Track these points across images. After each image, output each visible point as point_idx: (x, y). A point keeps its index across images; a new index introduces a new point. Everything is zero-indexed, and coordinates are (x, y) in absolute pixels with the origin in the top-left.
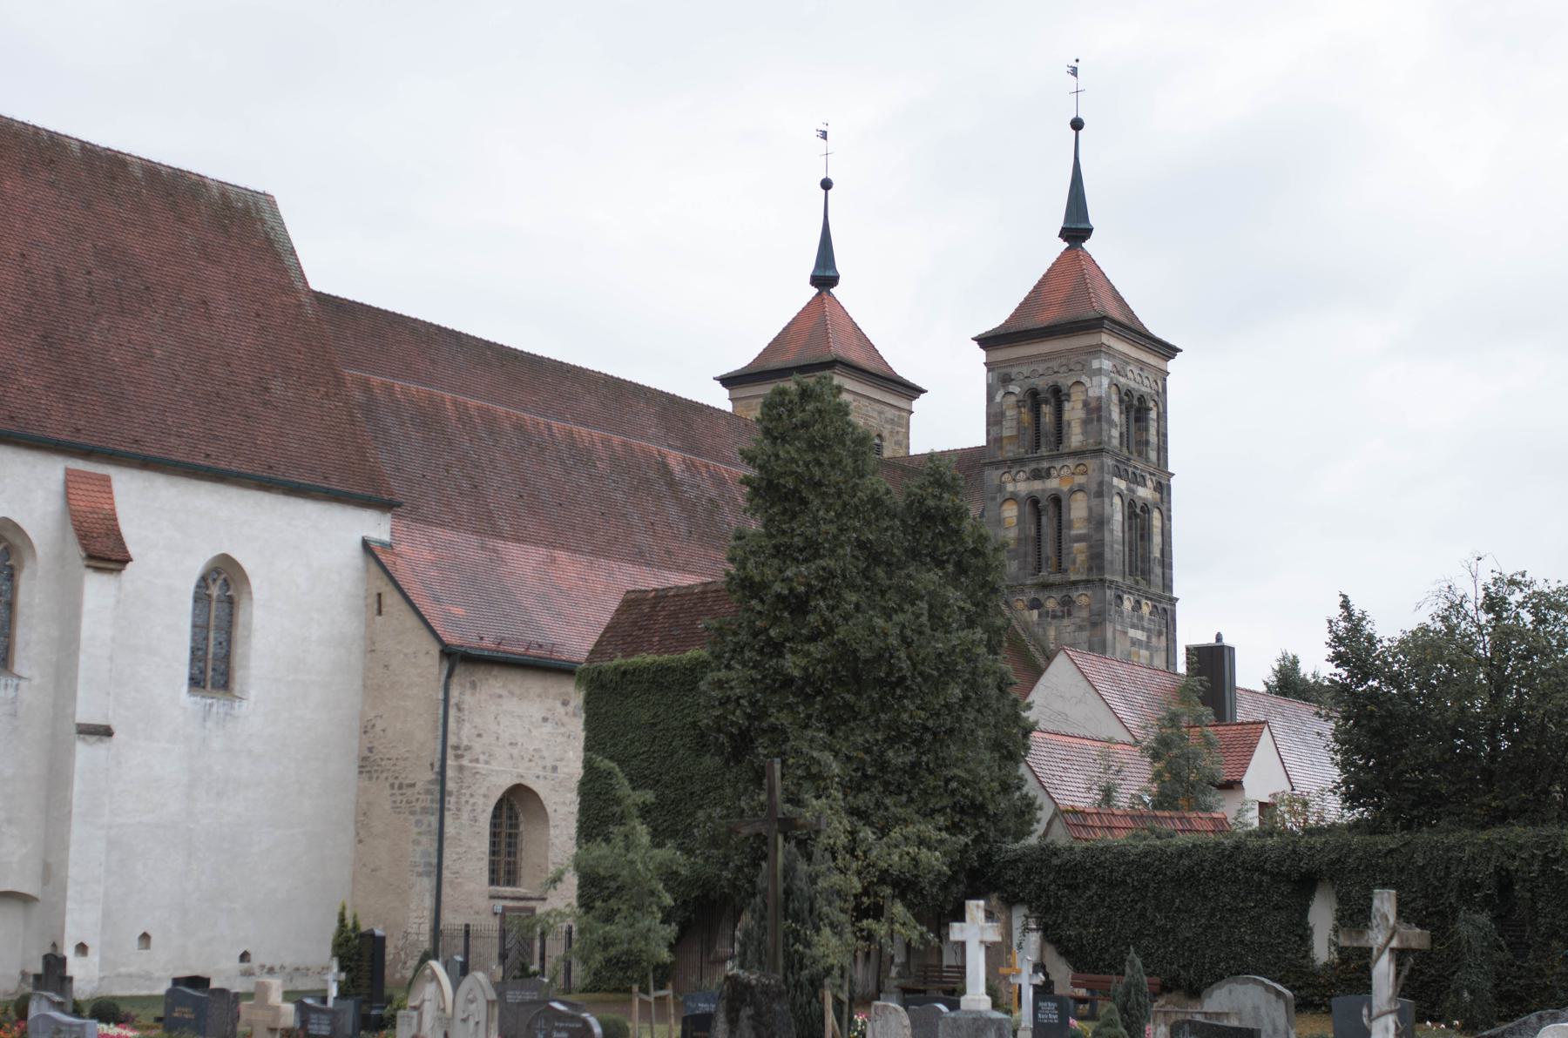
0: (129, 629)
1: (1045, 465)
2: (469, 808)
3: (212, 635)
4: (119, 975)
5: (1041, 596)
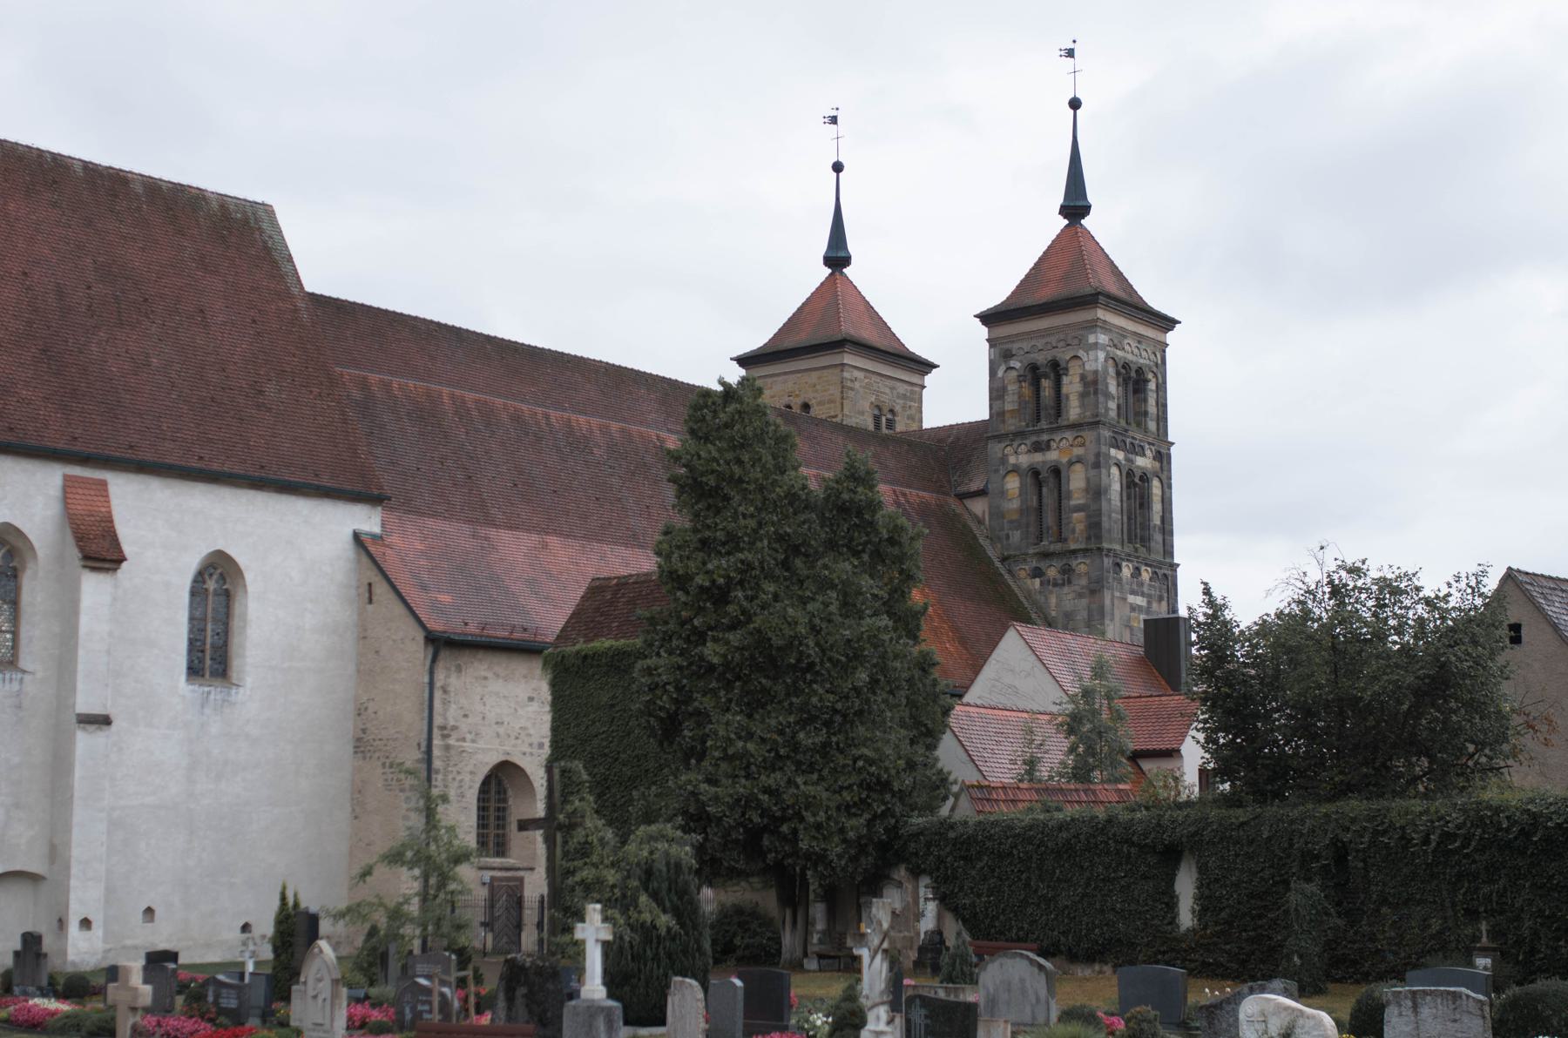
0: (126, 625)
1: (1045, 437)
2: (456, 784)
3: (209, 627)
4: (124, 947)
5: (1042, 565)
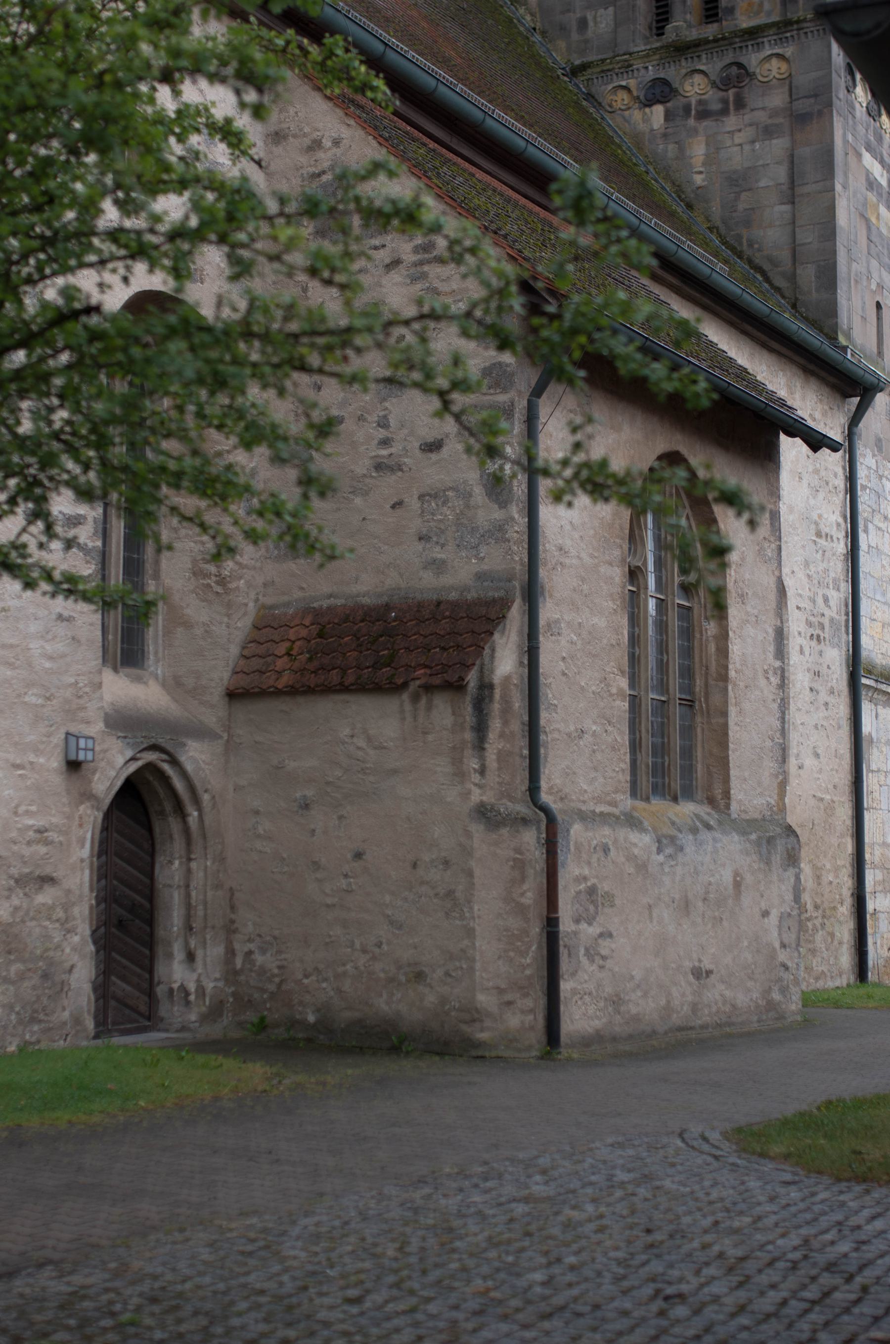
5: (671, 73)
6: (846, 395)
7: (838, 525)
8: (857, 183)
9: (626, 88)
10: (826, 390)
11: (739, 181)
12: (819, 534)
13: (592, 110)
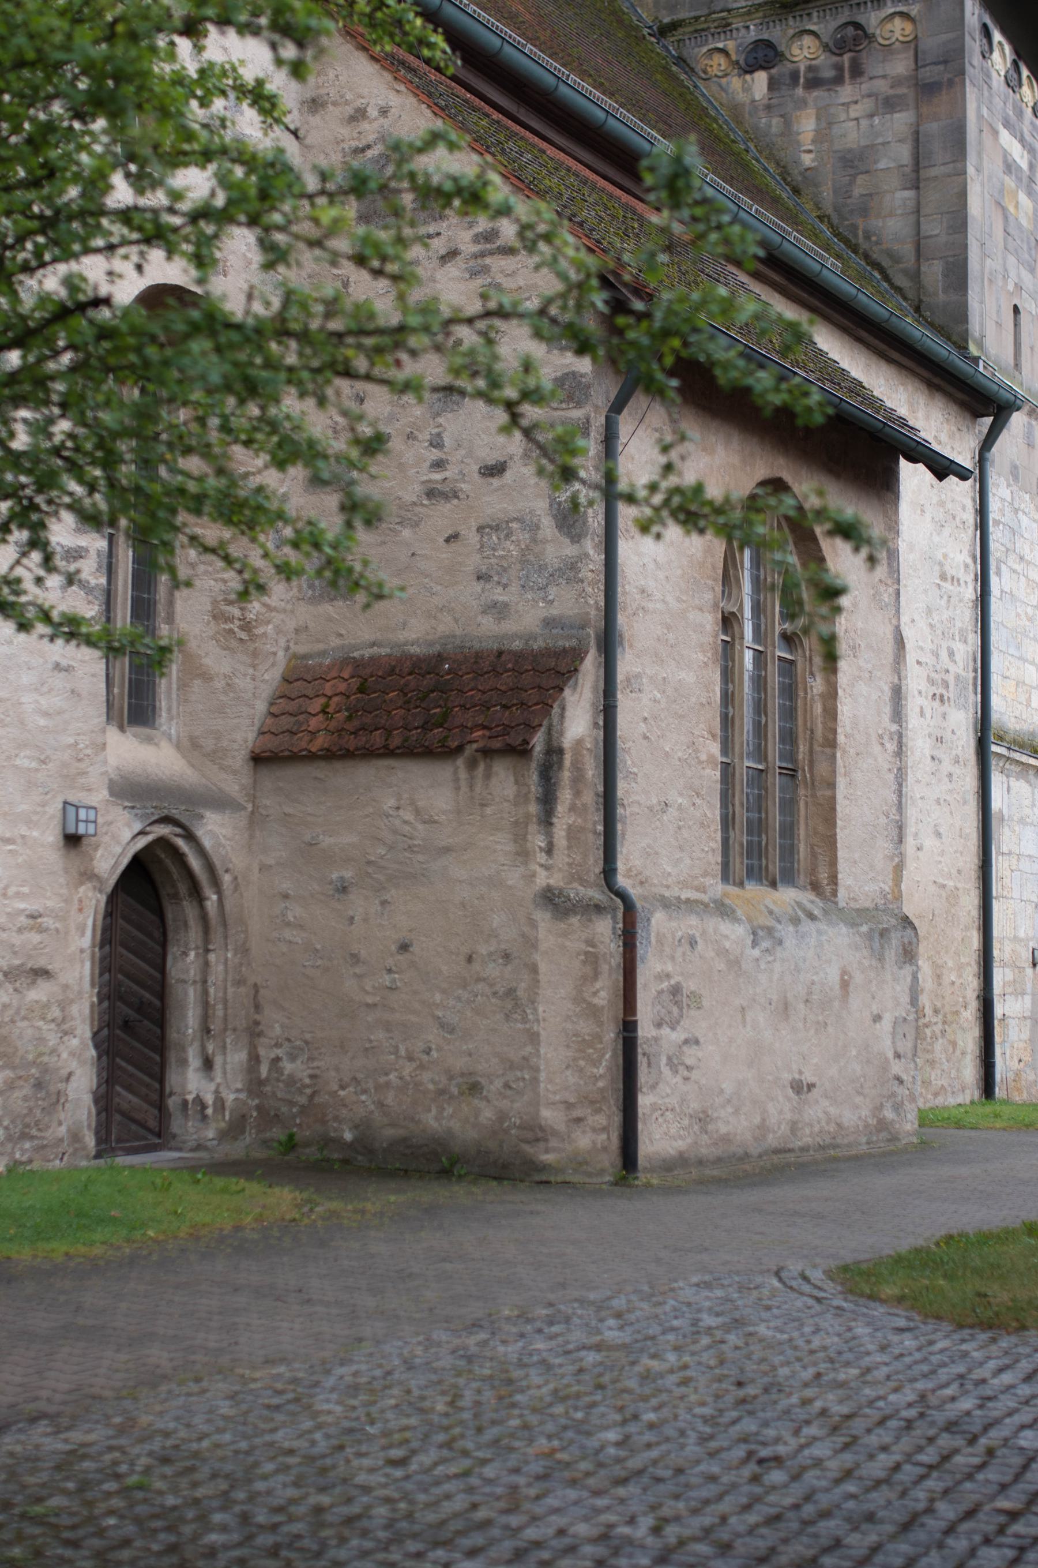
5: (776, 34)
6: (976, 415)
7: (966, 566)
8: (993, 165)
9: (723, 51)
10: (954, 409)
11: (854, 162)
12: (943, 577)
13: (683, 77)
